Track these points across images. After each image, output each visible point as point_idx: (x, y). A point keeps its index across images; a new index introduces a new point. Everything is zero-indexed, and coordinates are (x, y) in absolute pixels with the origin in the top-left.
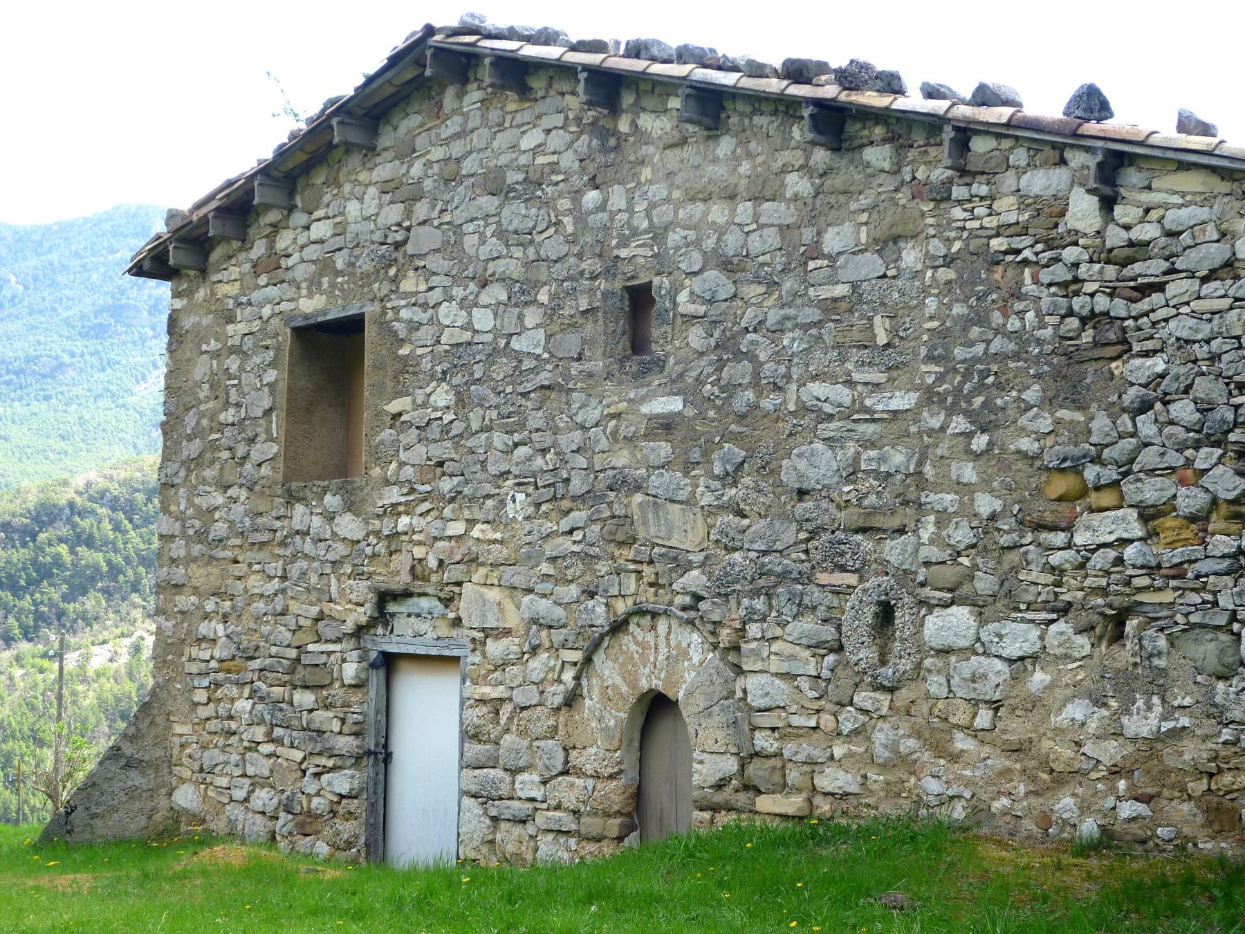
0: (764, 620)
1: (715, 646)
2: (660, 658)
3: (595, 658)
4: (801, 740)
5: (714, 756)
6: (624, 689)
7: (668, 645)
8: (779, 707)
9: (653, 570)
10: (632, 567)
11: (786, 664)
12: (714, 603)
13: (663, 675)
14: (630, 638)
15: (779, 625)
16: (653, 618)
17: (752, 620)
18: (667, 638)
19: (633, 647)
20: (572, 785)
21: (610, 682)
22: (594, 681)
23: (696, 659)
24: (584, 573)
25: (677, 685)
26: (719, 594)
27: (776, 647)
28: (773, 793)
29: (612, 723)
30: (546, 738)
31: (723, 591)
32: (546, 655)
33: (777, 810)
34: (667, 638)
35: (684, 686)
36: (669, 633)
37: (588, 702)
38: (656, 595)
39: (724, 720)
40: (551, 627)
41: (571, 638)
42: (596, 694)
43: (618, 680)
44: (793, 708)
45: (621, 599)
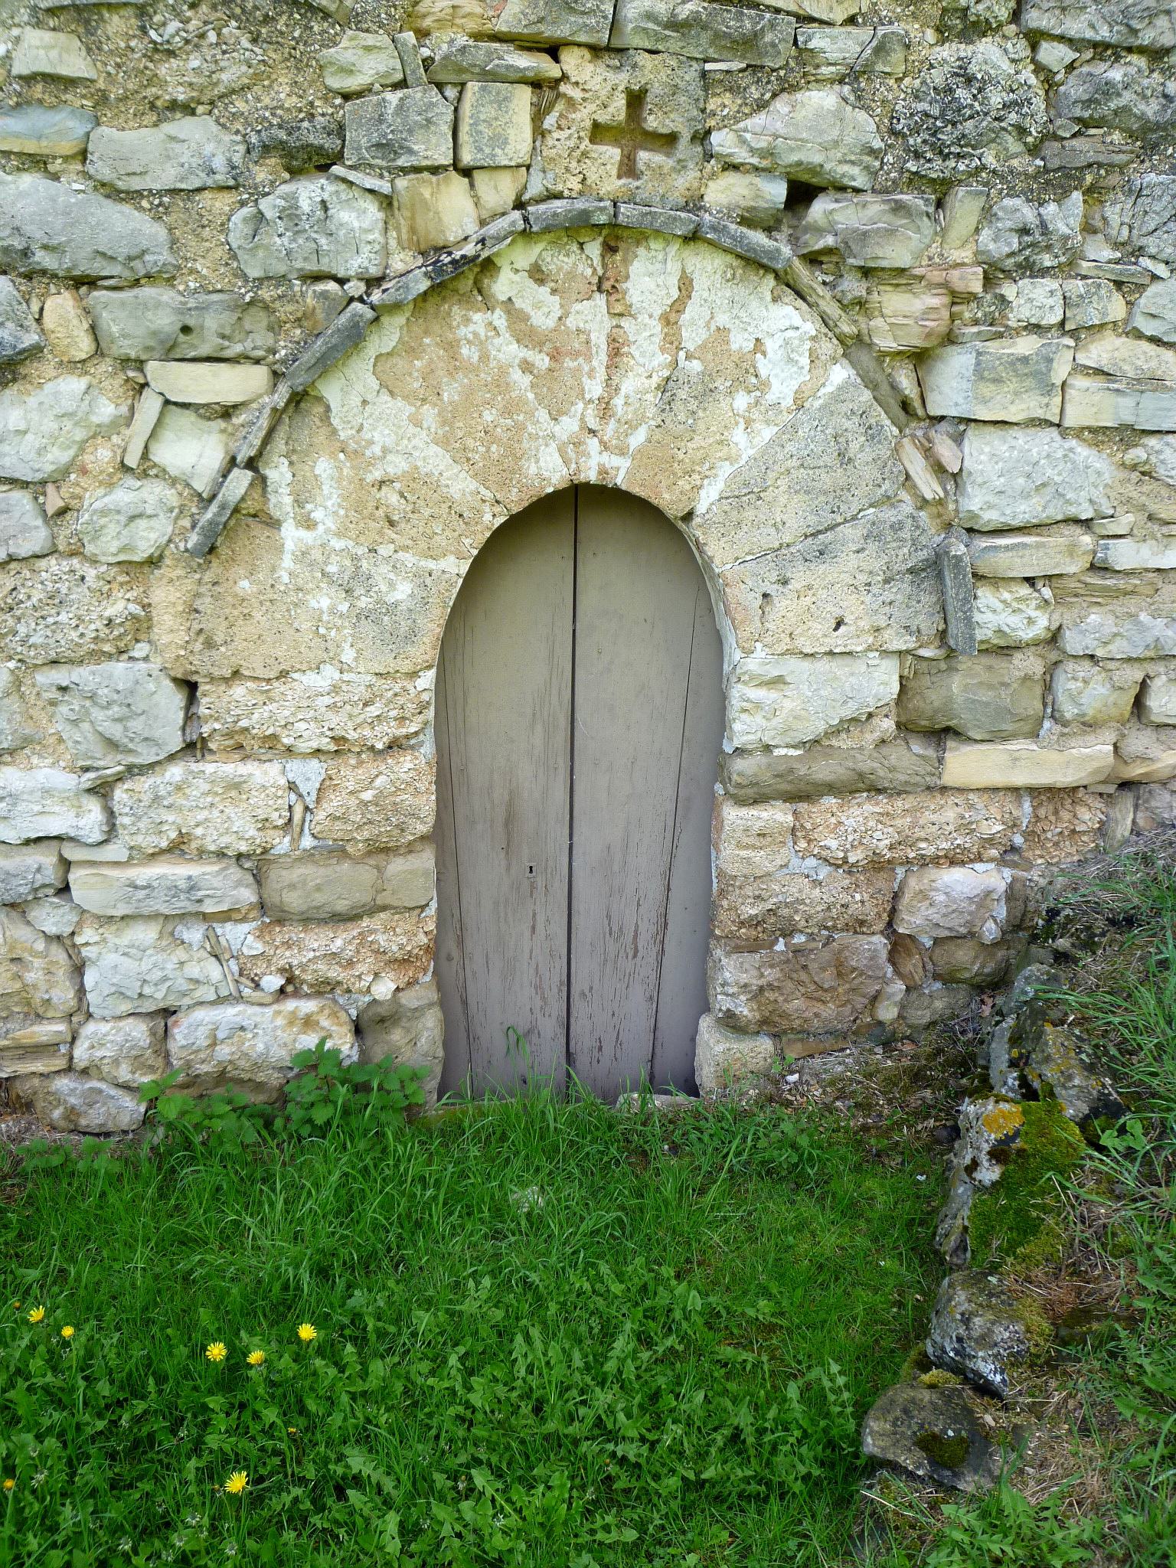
0: (1068, 268)
1: (854, 346)
2: (629, 385)
3: (331, 391)
4: (1131, 604)
5: (823, 665)
6: (461, 485)
7: (672, 340)
8: (1077, 521)
9: (622, 79)
10: (523, 61)
11: (1128, 402)
12: (899, 208)
13: (638, 439)
14: (499, 318)
15: (1119, 284)
16: (610, 249)
17: (1029, 269)
18: (671, 318)
19: (508, 350)
20: (236, 786)
21: (396, 465)
22: (323, 467)
23: (783, 386)
24: (260, 77)
25: (699, 469)
26: (915, 180)
27: (1100, 352)
28: (1005, 738)
29: (403, 592)
30: (97, 656)
31: (936, 168)
32: (75, 384)
33: (1020, 779)
34: (671, 318)
35: (725, 470)
36: (678, 306)
37: (291, 534)
38: (629, 168)
39: (878, 565)
40: (84, 282)
41: (212, 322)
42: (326, 512)
43: (436, 460)
44: (1125, 521)
45: (459, 183)
